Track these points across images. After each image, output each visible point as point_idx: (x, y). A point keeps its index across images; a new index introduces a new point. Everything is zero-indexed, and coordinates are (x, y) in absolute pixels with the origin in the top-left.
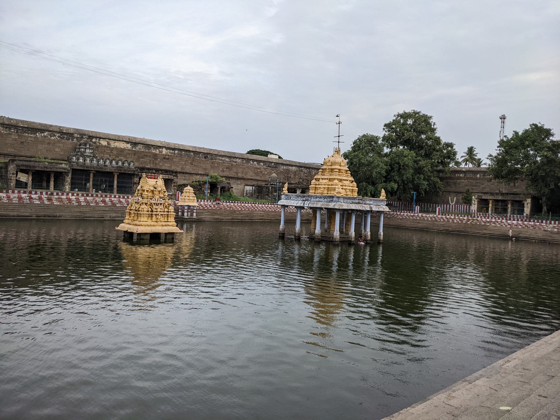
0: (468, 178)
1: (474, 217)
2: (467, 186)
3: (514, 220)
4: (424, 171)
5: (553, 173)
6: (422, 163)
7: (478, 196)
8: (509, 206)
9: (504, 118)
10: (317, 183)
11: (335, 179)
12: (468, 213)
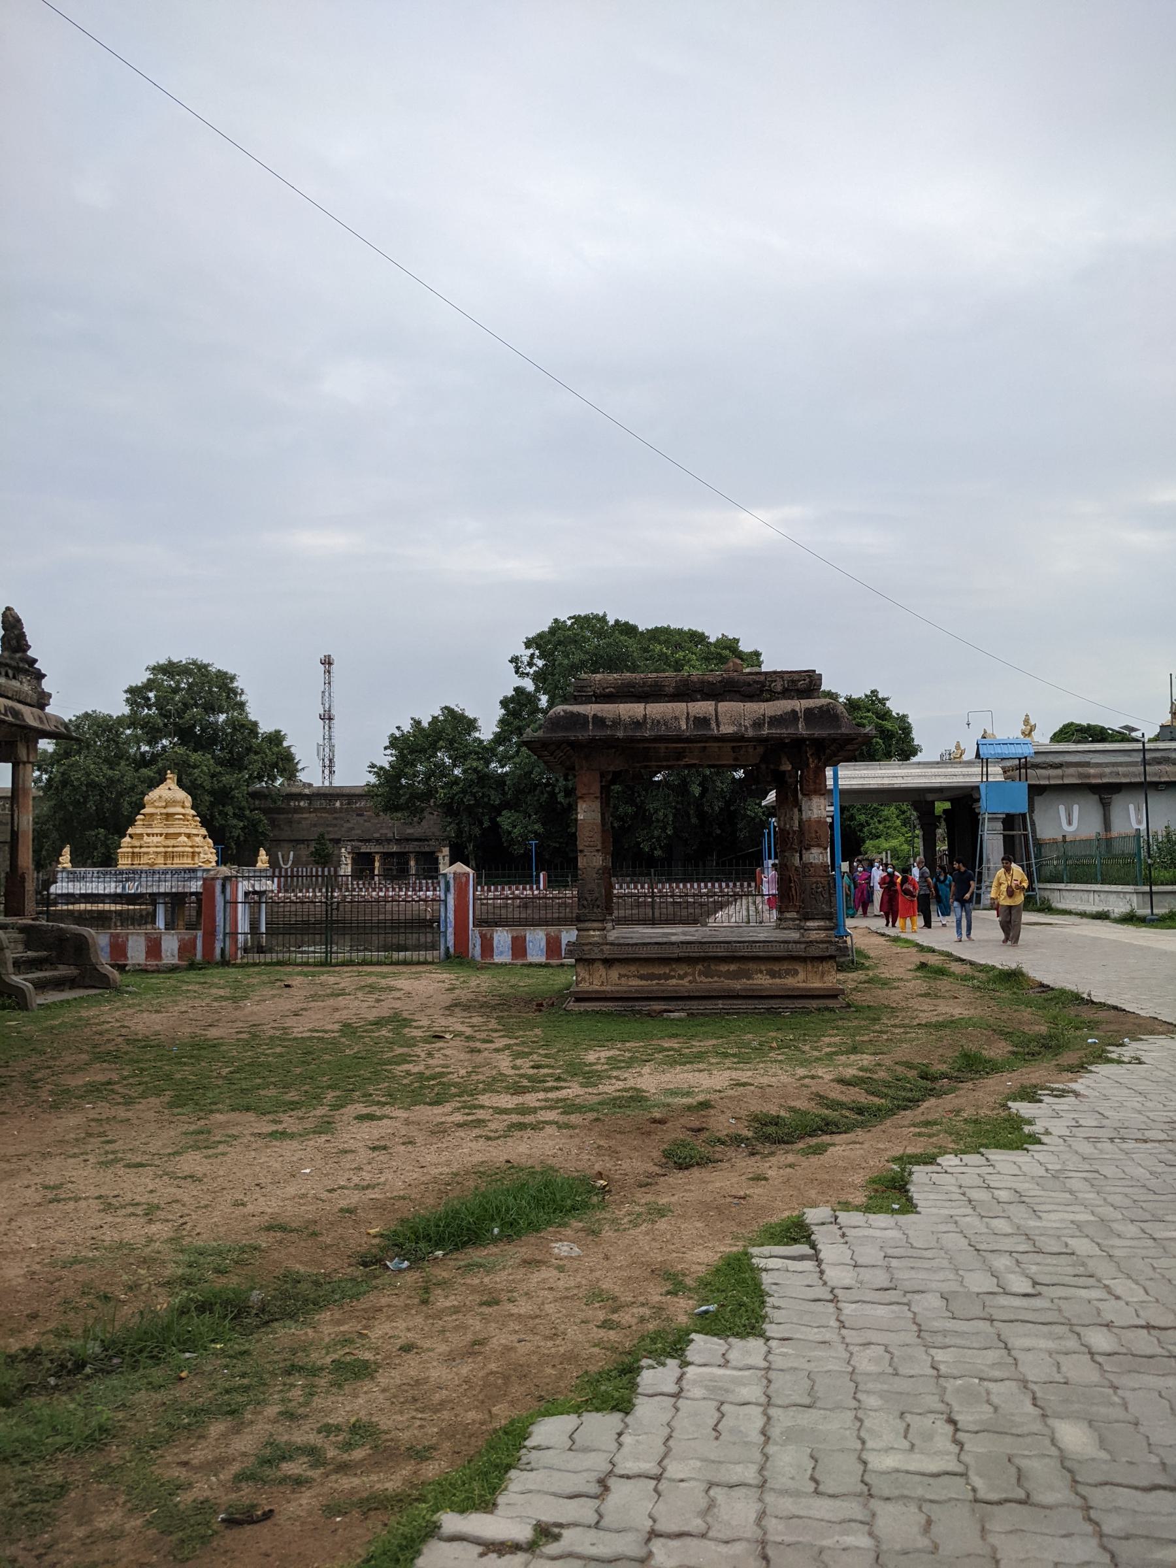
0: (316, 810)
1: (354, 890)
2: (315, 825)
3: (428, 890)
4: (233, 797)
5: (486, 800)
6: (228, 779)
7: (353, 847)
8: (412, 863)
9: (330, 664)
10: (137, 843)
11: (180, 834)
12: (332, 882)
